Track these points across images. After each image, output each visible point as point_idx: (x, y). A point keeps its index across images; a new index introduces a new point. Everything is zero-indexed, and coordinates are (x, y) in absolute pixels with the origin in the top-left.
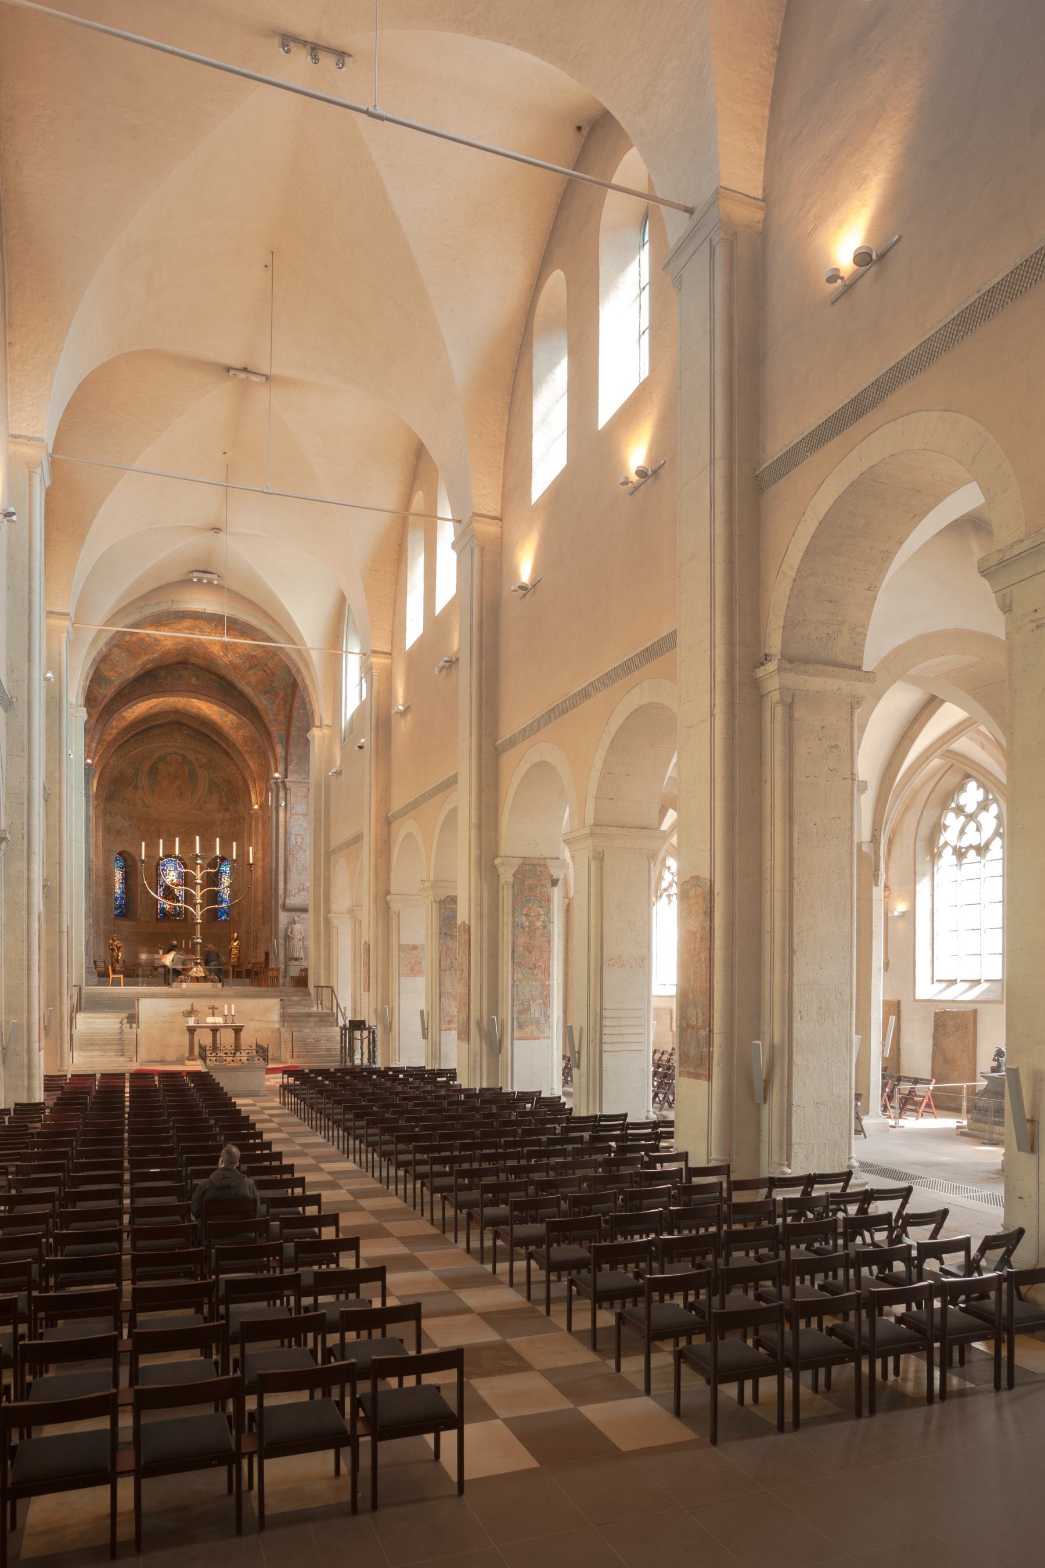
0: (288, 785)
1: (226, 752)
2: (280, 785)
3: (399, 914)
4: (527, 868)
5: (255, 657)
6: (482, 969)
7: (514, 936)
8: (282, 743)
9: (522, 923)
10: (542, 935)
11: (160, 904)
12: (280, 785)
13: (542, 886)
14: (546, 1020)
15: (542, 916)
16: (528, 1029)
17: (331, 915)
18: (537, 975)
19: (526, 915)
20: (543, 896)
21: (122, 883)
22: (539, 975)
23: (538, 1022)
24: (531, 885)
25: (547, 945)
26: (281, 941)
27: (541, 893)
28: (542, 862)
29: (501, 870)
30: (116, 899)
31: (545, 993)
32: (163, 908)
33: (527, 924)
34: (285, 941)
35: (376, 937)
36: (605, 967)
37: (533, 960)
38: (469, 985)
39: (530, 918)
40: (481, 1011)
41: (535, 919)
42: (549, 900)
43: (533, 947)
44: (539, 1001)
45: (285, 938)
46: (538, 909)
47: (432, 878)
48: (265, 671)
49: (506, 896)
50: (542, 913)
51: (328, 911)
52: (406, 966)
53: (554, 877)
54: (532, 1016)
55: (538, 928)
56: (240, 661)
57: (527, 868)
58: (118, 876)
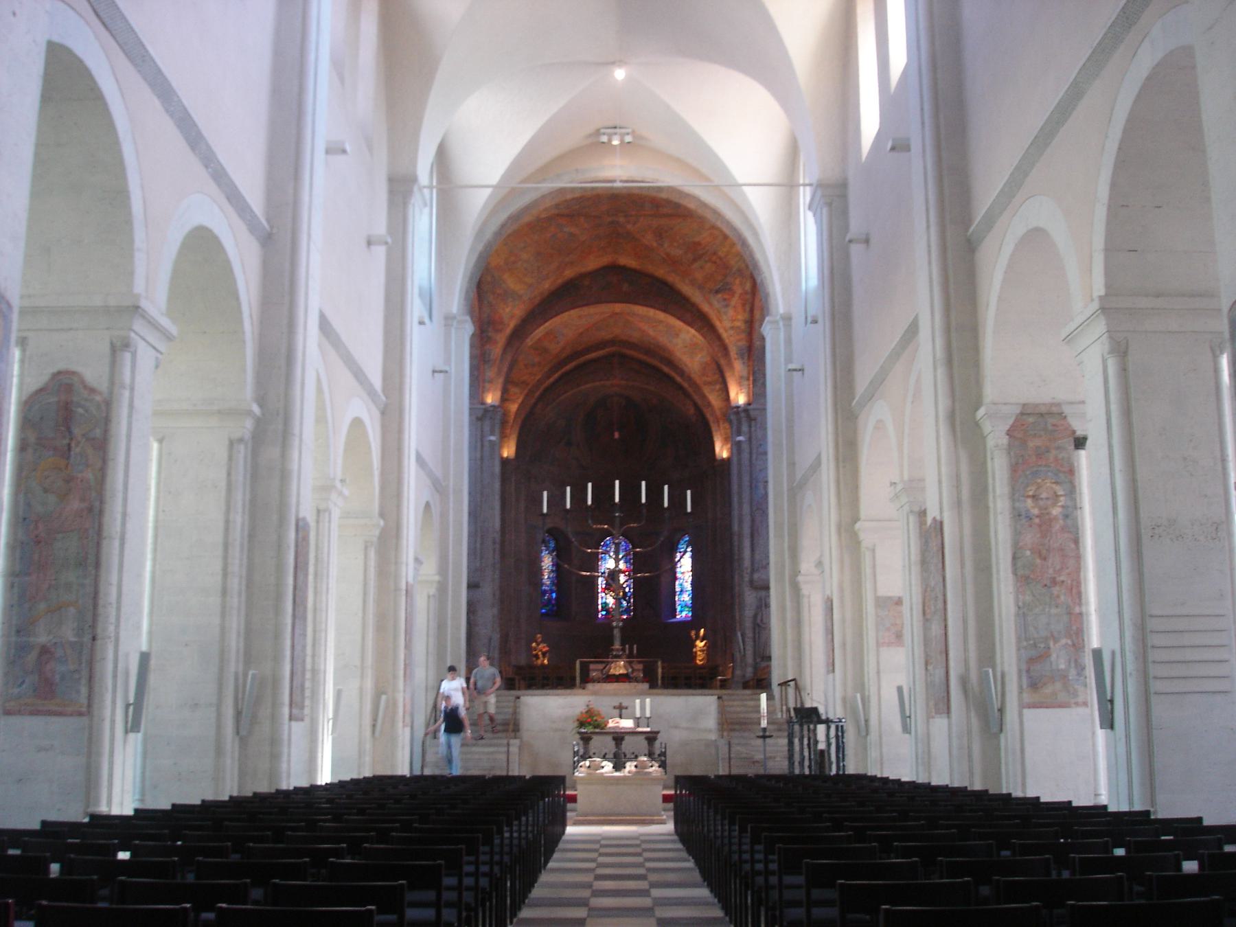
0: (752, 413)
1: (681, 388)
2: (743, 415)
3: (874, 551)
5: (699, 244)
6: (964, 589)
7: (1017, 534)
8: (743, 358)
9: (1028, 511)
10: (1064, 529)
11: (602, 598)
12: (743, 415)
13: (1058, 448)
14: (1079, 674)
15: (1062, 498)
16: (1048, 690)
17: (800, 578)
18: (1058, 597)
19: (1033, 497)
21: (552, 571)
22: (1062, 598)
23: (1064, 677)
24: (1038, 447)
25: (1073, 546)
26: (749, 634)
27: (1056, 459)
28: (1054, 409)
29: (987, 427)
30: (545, 592)
31: (1074, 628)
32: (605, 603)
33: (1036, 511)
34: (754, 633)
35: (841, 590)
36: (1145, 539)
37: (1051, 571)
38: (945, 620)
39: (1041, 503)
40: (966, 661)
41: (1049, 502)
42: (1071, 472)
43: (1048, 550)
44: (1064, 641)
45: (754, 629)
46: (1054, 486)
47: (906, 477)
48: (715, 263)
49: (999, 468)
51: (796, 572)
52: (888, 629)
55: (1056, 518)
56: (681, 252)
58: (546, 562)
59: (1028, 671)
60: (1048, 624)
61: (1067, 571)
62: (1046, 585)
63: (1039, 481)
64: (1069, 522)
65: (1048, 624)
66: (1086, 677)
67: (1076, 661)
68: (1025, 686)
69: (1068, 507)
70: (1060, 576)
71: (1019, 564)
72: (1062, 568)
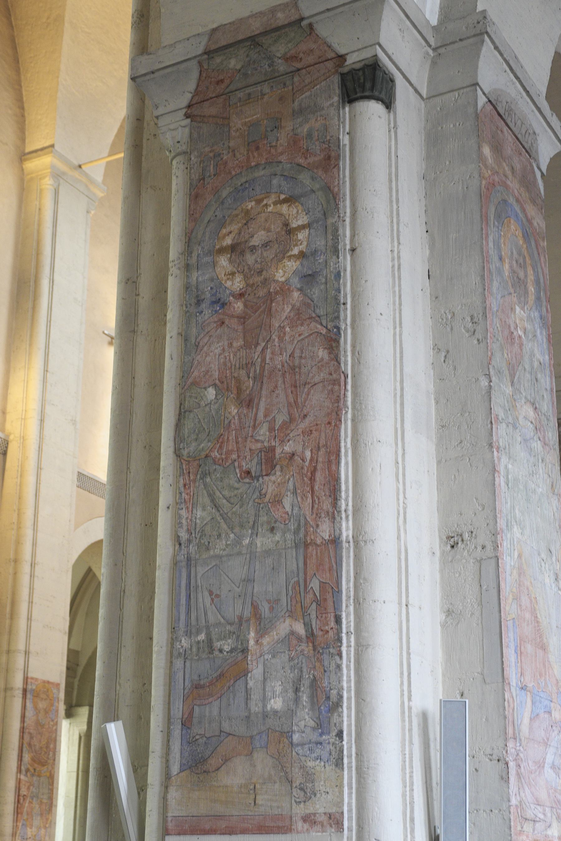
4: (233, 63)
13: (295, 114)
15: (302, 236)
18: (278, 501)
20: (306, 153)
22: (287, 502)
25: (322, 353)
31: (315, 585)
37: (263, 431)
39: (250, 259)
41: (269, 254)
43: (259, 379)
46: (284, 209)
50: (303, 220)
53: (351, 60)
54: (255, 707)
57: (233, 63)
59: (186, 724)
60: (249, 580)
61: (303, 425)
62: (248, 473)
63: (251, 205)
64: (316, 292)
65: (249, 580)
66: (340, 735)
67: (314, 683)
68: (175, 769)
69: (314, 253)
70: (282, 442)
71: (189, 425)
72: (292, 420)
